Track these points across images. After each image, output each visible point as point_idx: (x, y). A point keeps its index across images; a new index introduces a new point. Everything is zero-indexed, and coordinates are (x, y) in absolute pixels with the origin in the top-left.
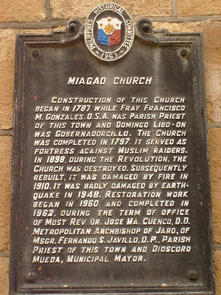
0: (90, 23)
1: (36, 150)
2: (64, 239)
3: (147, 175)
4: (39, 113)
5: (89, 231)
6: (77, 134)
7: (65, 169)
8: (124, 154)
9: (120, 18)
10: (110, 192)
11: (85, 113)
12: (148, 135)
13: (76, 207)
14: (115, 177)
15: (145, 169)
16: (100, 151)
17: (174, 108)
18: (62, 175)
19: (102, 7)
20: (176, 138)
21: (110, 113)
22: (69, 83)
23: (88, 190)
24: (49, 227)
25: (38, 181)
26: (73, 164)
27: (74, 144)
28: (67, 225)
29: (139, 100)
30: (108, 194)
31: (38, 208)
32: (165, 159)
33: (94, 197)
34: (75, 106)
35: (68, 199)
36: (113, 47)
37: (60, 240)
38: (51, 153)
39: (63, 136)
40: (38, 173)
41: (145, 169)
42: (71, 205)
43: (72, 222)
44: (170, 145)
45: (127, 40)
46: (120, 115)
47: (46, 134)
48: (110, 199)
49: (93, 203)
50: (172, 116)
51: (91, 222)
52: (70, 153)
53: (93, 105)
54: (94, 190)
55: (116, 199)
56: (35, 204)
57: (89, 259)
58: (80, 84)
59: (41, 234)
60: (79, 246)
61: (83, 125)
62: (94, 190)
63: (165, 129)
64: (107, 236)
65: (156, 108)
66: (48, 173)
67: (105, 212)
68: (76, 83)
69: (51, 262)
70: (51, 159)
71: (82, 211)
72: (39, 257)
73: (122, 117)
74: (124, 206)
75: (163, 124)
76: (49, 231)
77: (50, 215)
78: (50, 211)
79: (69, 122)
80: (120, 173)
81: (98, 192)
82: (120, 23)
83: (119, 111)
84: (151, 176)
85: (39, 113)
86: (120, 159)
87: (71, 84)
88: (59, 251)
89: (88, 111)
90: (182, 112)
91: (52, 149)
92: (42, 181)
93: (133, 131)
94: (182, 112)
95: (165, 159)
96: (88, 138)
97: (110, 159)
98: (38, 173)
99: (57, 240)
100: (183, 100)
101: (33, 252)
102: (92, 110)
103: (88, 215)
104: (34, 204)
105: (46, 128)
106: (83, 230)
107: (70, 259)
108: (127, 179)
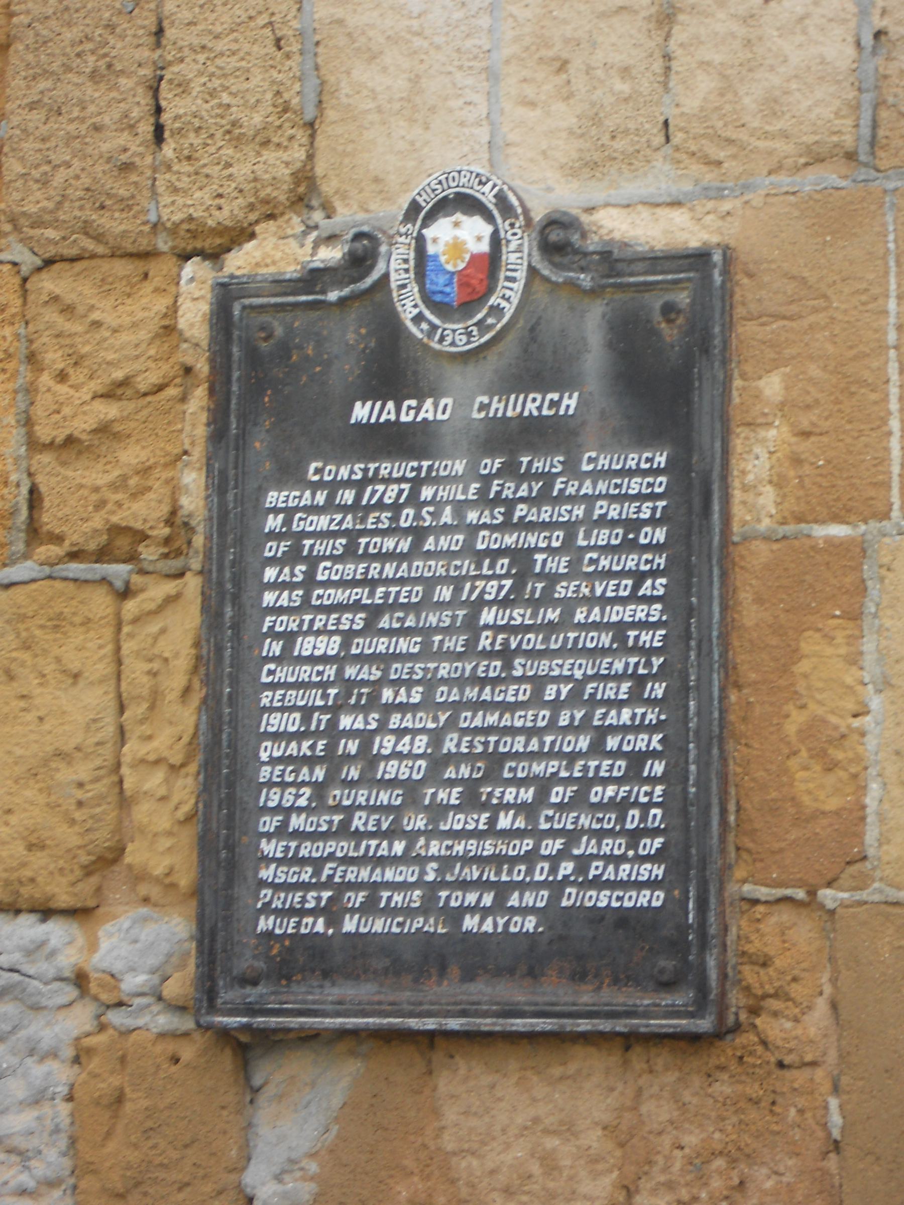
0: (407, 235)
1: (268, 620)
2: (335, 869)
3: (555, 687)
4: (276, 511)
5: (399, 847)
6: (371, 572)
7: (340, 672)
8: (497, 629)
9: (489, 217)
10: (455, 736)
11: (396, 508)
12: (562, 570)
13: (368, 780)
14: (471, 693)
15: (551, 669)
16: (433, 619)
17: (635, 485)
18: (333, 692)
19: (440, 183)
20: (639, 577)
21: (460, 507)
22: (353, 421)
23: (400, 733)
24: (298, 835)
25: (271, 710)
26: (361, 659)
27: (364, 601)
28: (344, 831)
29: (541, 464)
30: (449, 745)
31: (270, 784)
32: (606, 640)
33: (416, 751)
34: (369, 489)
35: (348, 758)
36: (467, 307)
37: (327, 872)
38: (305, 628)
39: (337, 578)
40: (273, 686)
41: (551, 669)
42: (354, 773)
43: (358, 822)
44: (622, 598)
45: (507, 284)
46: (487, 513)
47: (293, 575)
48: (455, 758)
49: (412, 768)
50: (630, 510)
51: (405, 822)
52: (355, 627)
53: (417, 483)
54: (414, 732)
55: (470, 757)
56: (265, 773)
57: (399, 924)
58: (382, 420)
59: (279, 855)
60: (374, 887)
61: (389, 544)
62: (414, 732)
63: (607, 549)
64: (446, 863)
65: (587, 488)
66: (299, 685)
67: (442, 795)
68: (373, 420)
69: (303, 931)
70: (306, 646)
71: (382, 793)
72: (272, 918)
73: (493, 517)
74: (492, 775)
75: (602, 536)
76: (298, 848)
77: (302, 802)
78: (302, 791)
79: (352, 535)
80: (483, 682)
81: (425, 738)
82: (488, 230)
83: (485, 501)
84: (565, 690)
85: (276, 511)
86: (484, 642)
87: (358, 424)
88: (323, 903)
89: (402, 501)
90: (659, 497)
91: (308, 617)
92: (282, 709)
93: (521, 558)
94: (659, 497)
95: (606, 640)
96: (402, 581)
97: (456, 643)
98: (273, 686)
99: (317, 873)
100: (661, 460)
101: (259, 905)
102: (414, 499)
103: (398, 802)
104: (262, 774)
105: (293, 556)
106: (385, 844)
107: (349, 925)
108: (500, 699)
